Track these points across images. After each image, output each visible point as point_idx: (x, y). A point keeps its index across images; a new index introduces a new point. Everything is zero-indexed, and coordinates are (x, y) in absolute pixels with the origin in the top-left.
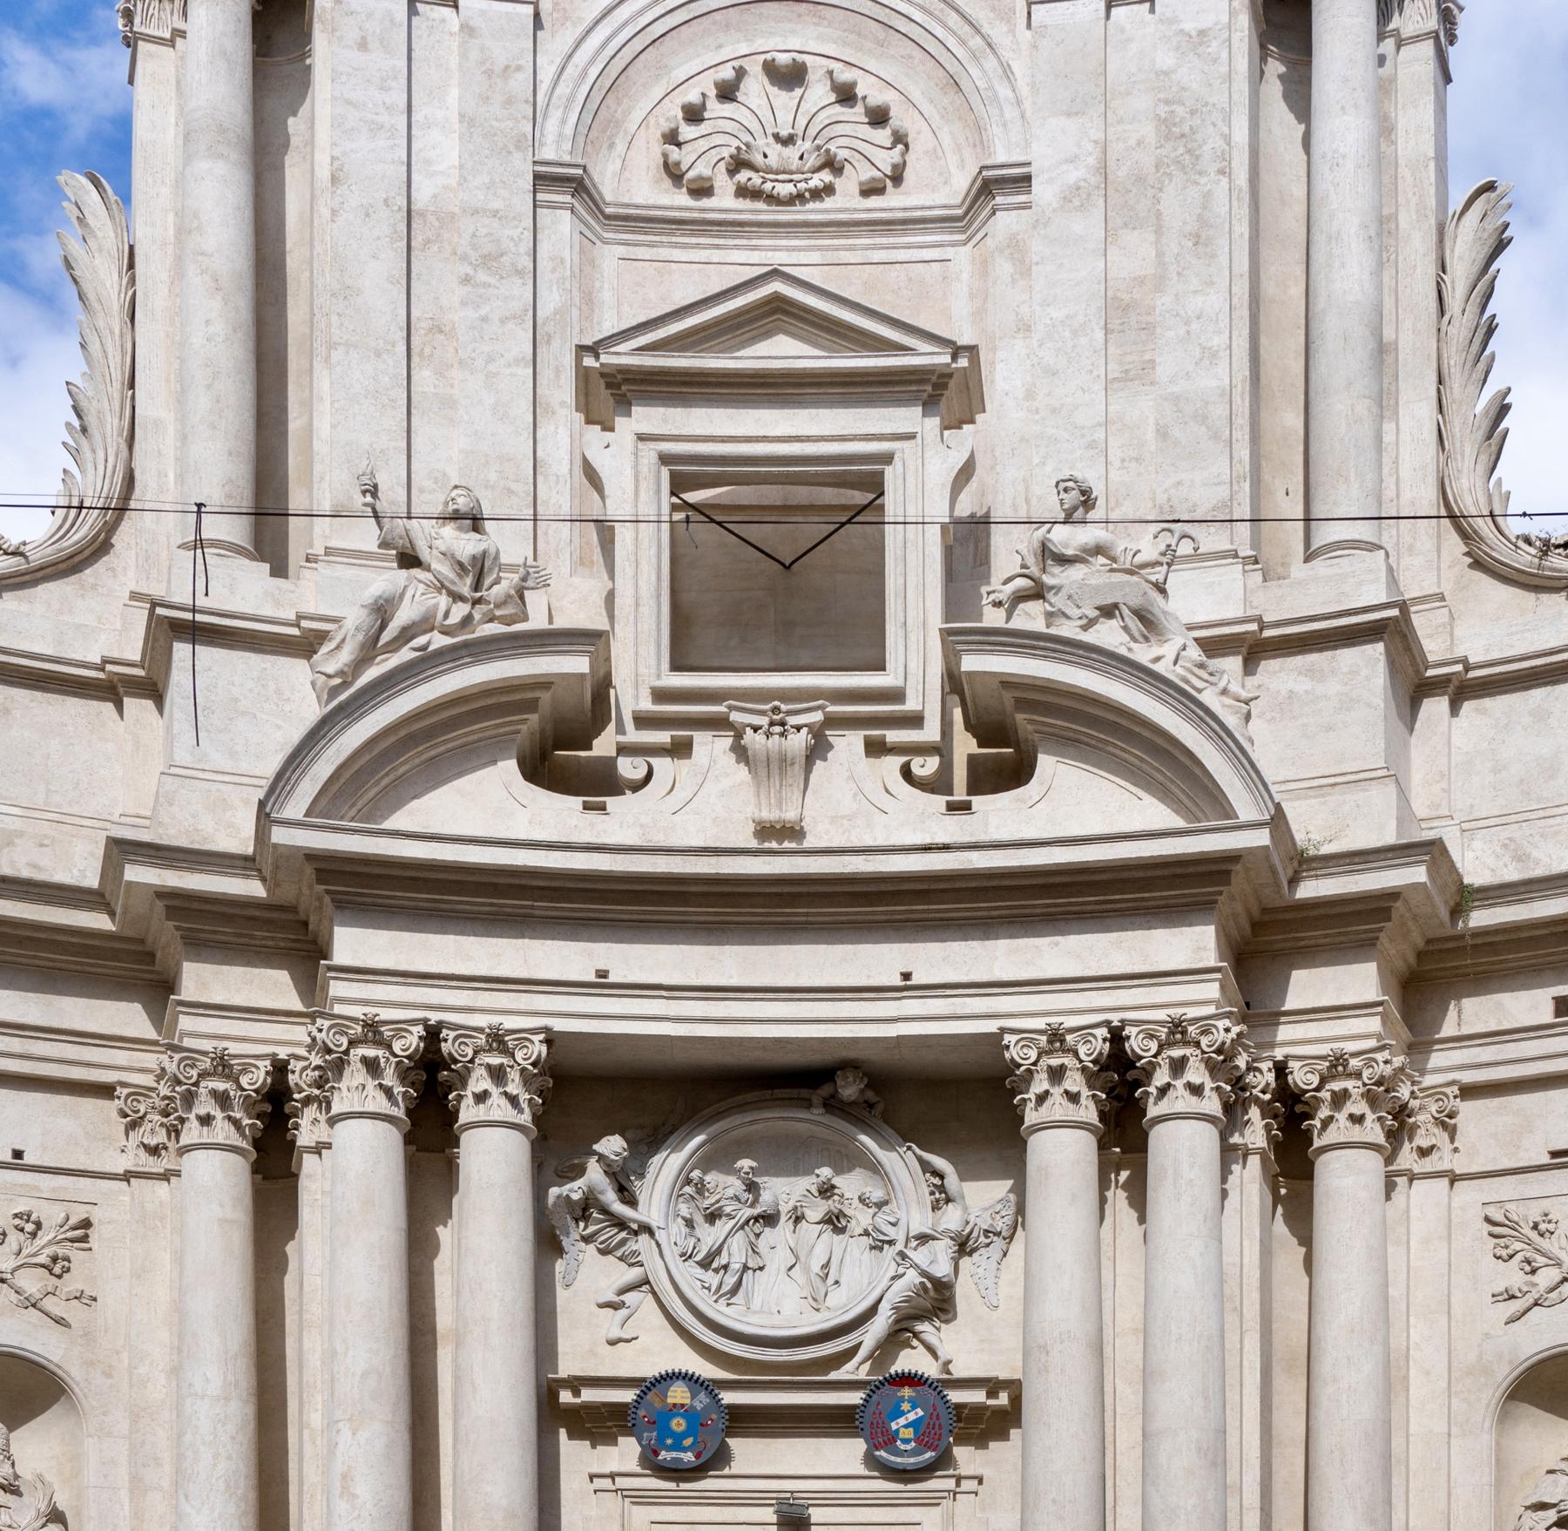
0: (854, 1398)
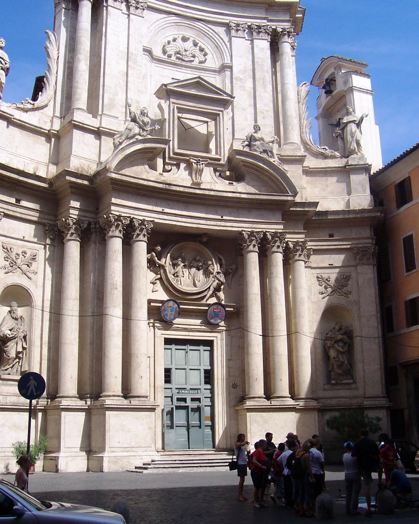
0: (207, 308)
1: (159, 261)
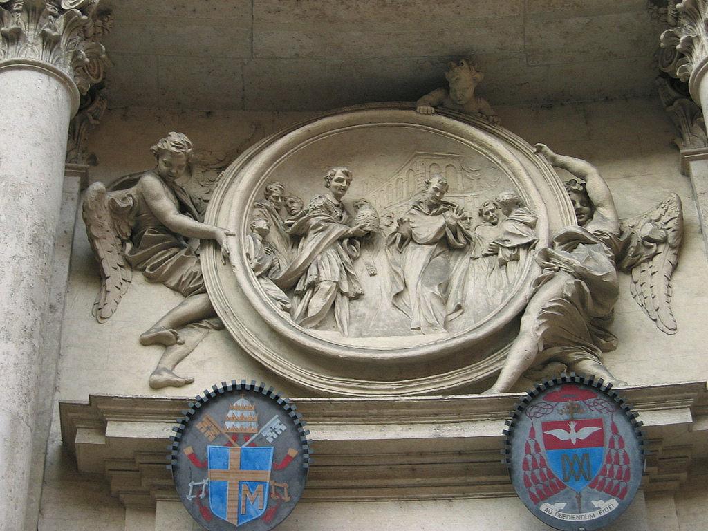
0: (496, 429)
1: (186, 221)
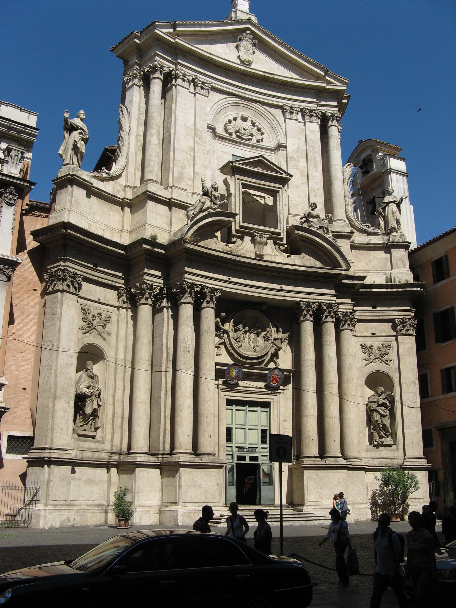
1: (222, 327)
